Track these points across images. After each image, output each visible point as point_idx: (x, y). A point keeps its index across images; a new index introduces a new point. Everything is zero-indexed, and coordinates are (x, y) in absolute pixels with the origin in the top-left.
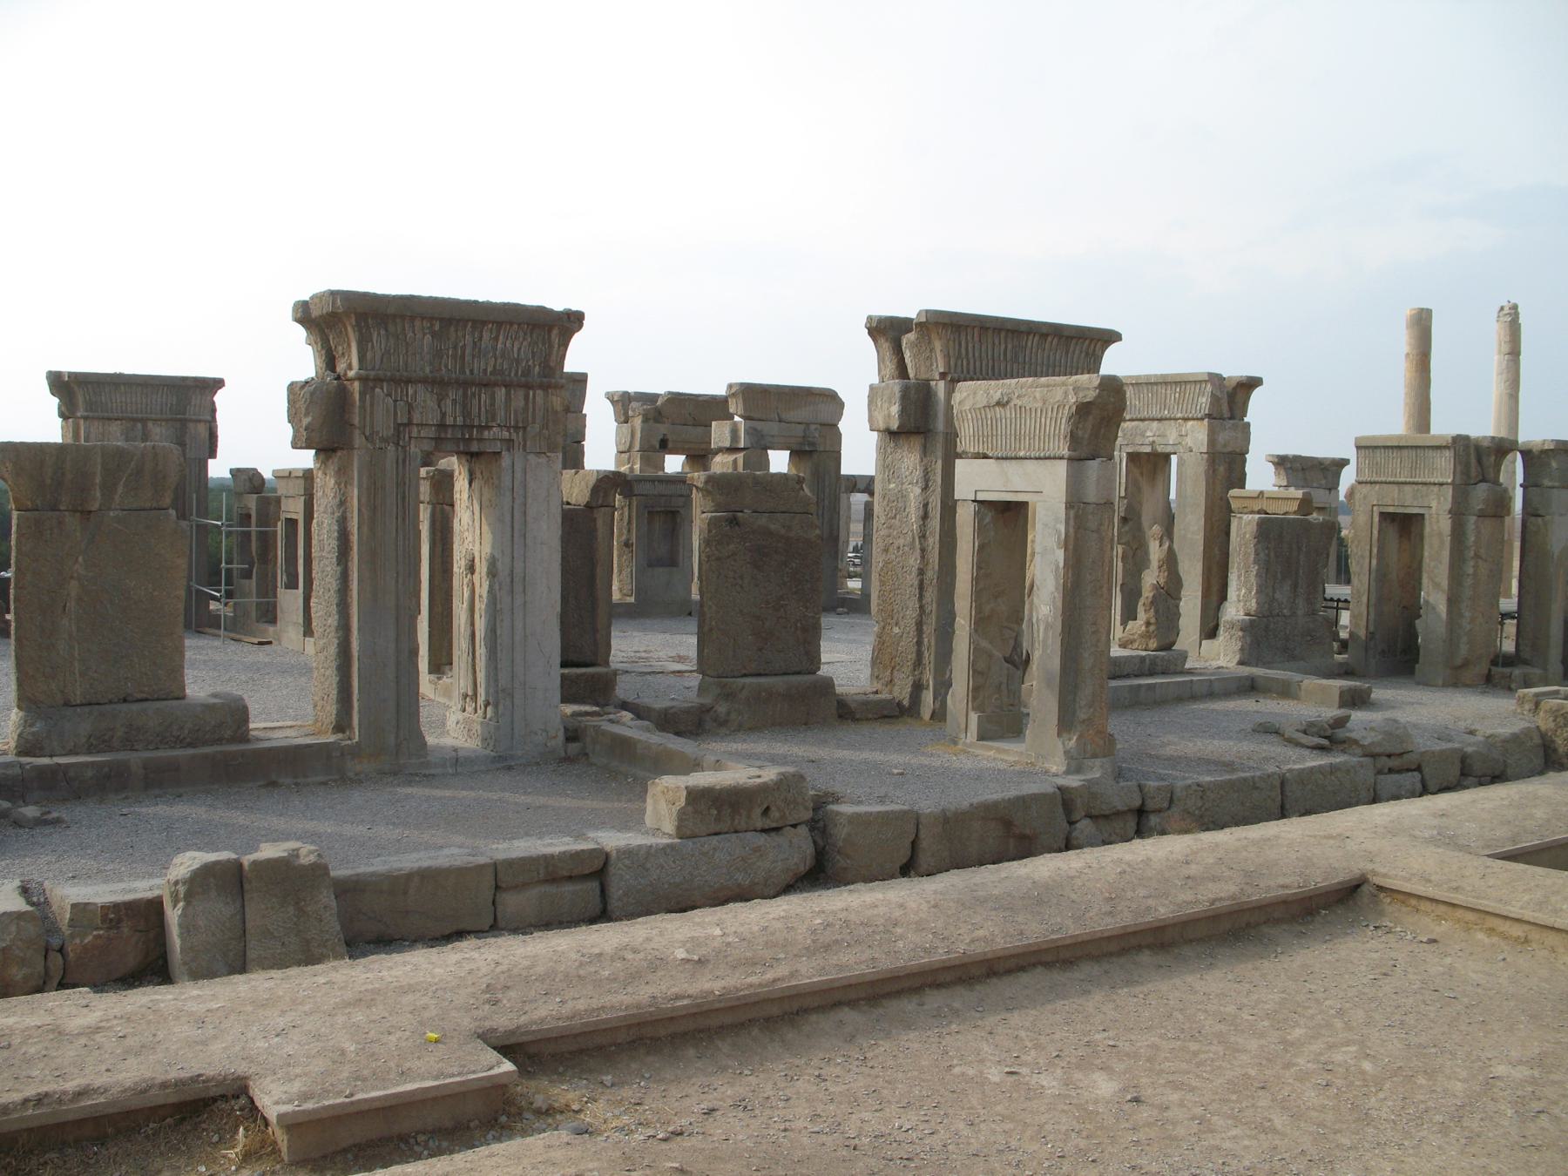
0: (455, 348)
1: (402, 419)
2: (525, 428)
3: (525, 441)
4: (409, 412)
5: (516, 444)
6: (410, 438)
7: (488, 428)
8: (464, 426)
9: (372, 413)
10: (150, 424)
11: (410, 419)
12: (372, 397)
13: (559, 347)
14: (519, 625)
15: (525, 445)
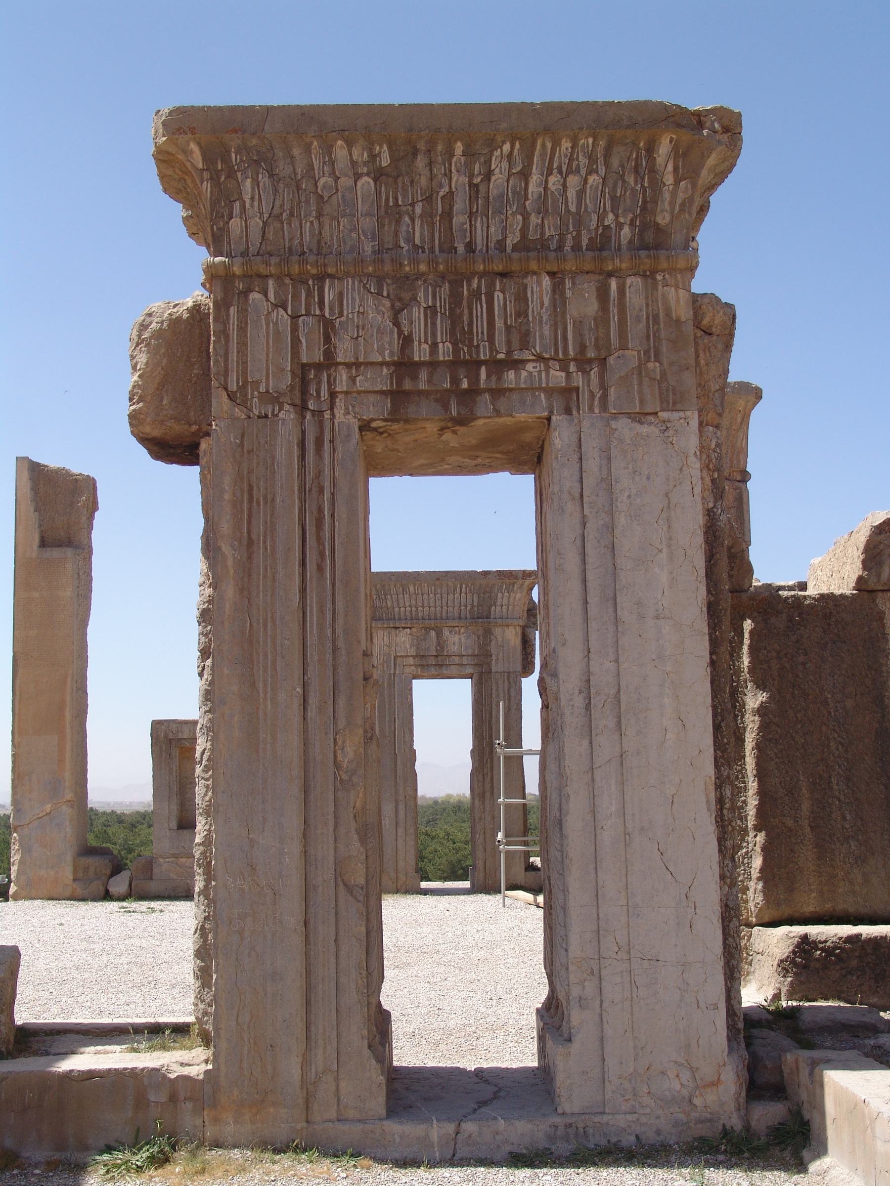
0: (429, 199)
1: (312, 353)
2: (603, 361)
3: (604, 387)
4: (327, 340)
5: (585, 397)
6: (333, 395)
7: (516, 365)
8: (455, 364)
9: (243, 345)
10: (446, 632)
11: (329, 354)
12: (243, 312)
13: (677, 182)
14: (608, 805)
15: (604, 399)
